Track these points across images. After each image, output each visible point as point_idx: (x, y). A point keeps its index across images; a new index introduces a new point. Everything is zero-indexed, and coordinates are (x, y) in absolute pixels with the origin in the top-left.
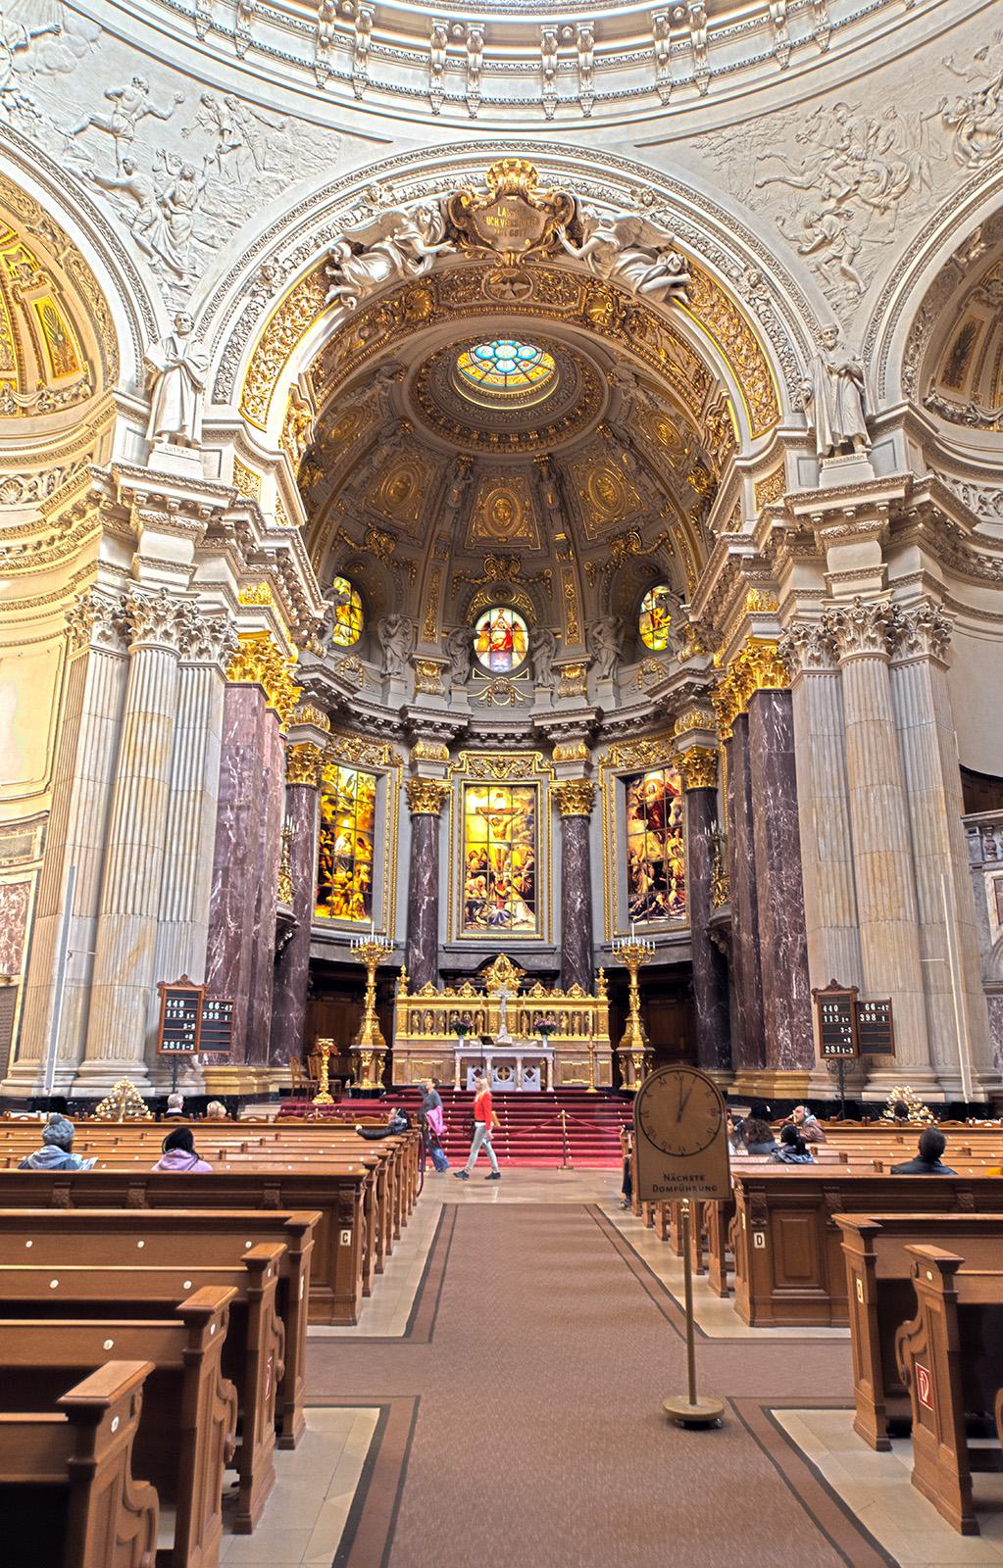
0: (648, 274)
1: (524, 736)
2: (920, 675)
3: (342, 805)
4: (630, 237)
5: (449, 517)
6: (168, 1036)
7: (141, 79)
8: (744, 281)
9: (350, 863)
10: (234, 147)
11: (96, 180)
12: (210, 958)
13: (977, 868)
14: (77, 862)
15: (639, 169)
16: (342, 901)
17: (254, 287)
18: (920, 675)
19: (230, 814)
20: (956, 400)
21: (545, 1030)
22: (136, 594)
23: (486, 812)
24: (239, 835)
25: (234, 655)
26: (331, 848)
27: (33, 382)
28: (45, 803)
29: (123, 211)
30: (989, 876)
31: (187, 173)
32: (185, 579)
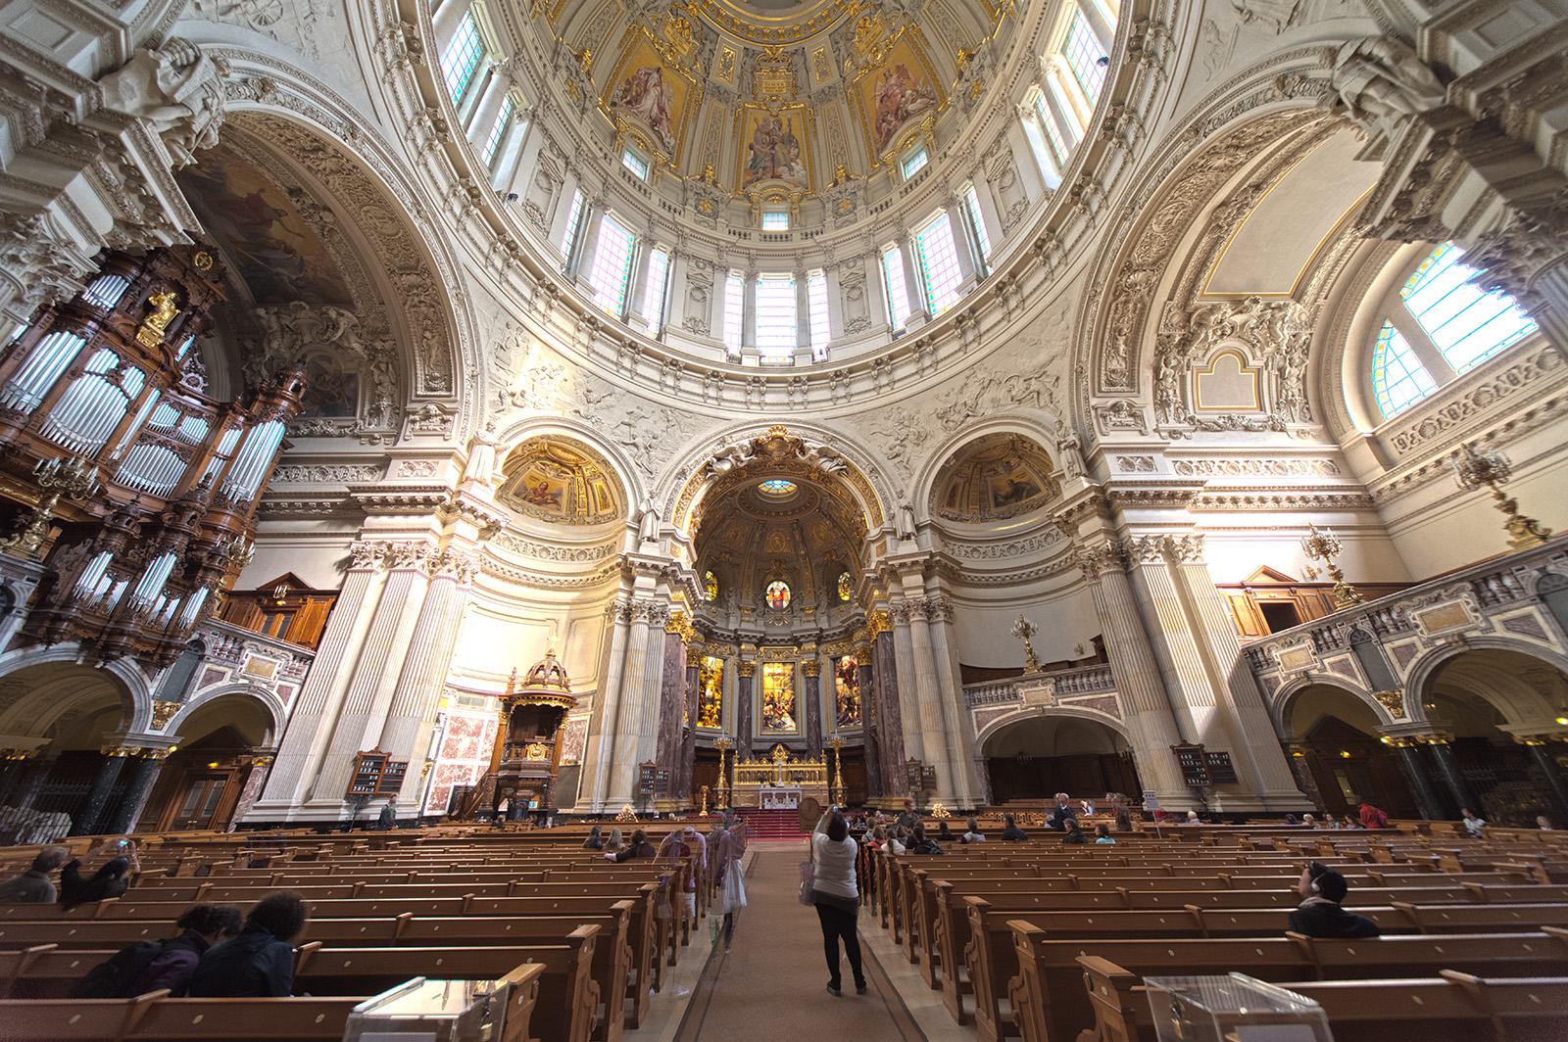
2: (941, 629)
3: (709, 674)
4: (823, 453)
5: (755, 545)
6: (643, 786)
8: (868, 471)
9: (712, 701)
12: (658, 751)
13: (969, 708)
14: (608, 712)
15: (826, 428)
18: (941, 629)
19: (667, 689)
20: (954, 511)
21: (799, 780)
22: (634, 602)
23: (773, 675)
25: (669, 622)
27: (592, 511)
28: (594, 687)
30: (973, 711)
32: (652, 594)
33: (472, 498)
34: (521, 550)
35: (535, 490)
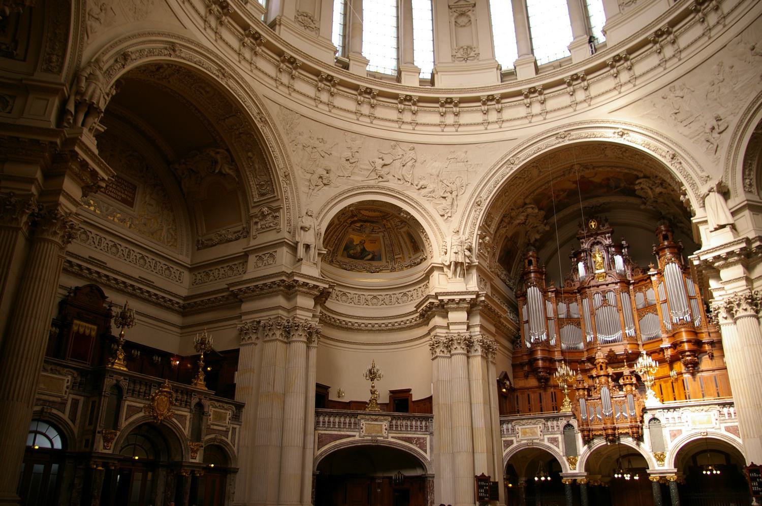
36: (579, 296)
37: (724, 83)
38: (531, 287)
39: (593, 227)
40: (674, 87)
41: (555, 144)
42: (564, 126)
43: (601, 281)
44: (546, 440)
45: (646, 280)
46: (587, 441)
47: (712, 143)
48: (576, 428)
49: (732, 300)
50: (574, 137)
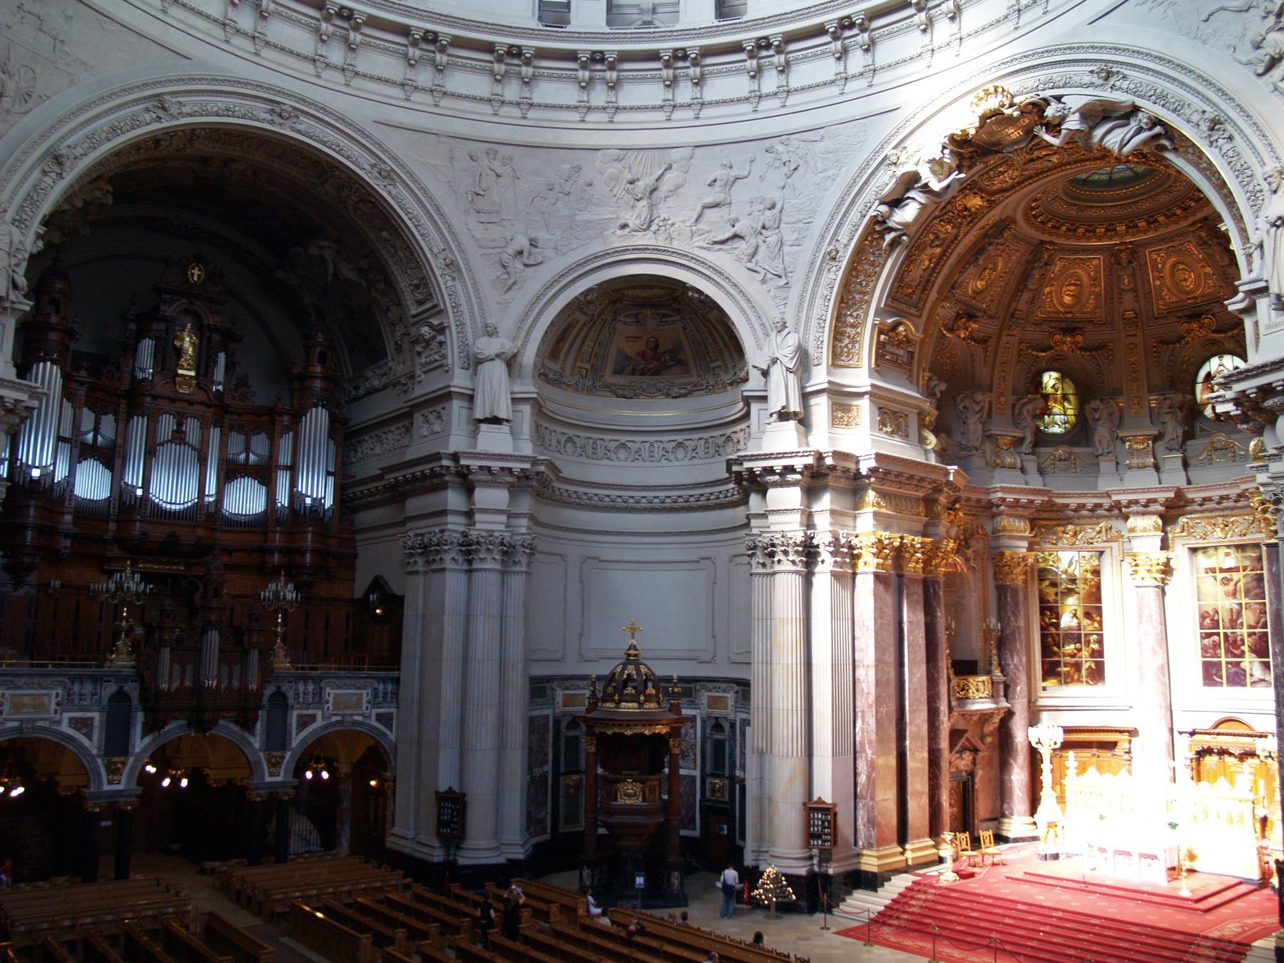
0: (1122, 140)
1: (1240, 496)
7: (725, 162)
8: (1204, 126)
10: (795, 169)
11: (715, 243)
16: (1073, 670)
17: (828, 267)
24: (868, 687)
26: (1057, 626)
29: (736, 252)
31: (768, 206)
33: (476, 456)
34: (646, 456)
35: (642, 354)
36: (123, 407)
37: (566, 198)
38: (45, 362)
39: (196, 279)
40: (496, 152)
41: (263, 120)
42: (291, 96)
43: (184, 390)
44: (65, 722)
45: (259, 416)
46: (148, 728)
47: (508, 273)
48: (135, 702)
49: (482, 540)
50: (302, 127)
